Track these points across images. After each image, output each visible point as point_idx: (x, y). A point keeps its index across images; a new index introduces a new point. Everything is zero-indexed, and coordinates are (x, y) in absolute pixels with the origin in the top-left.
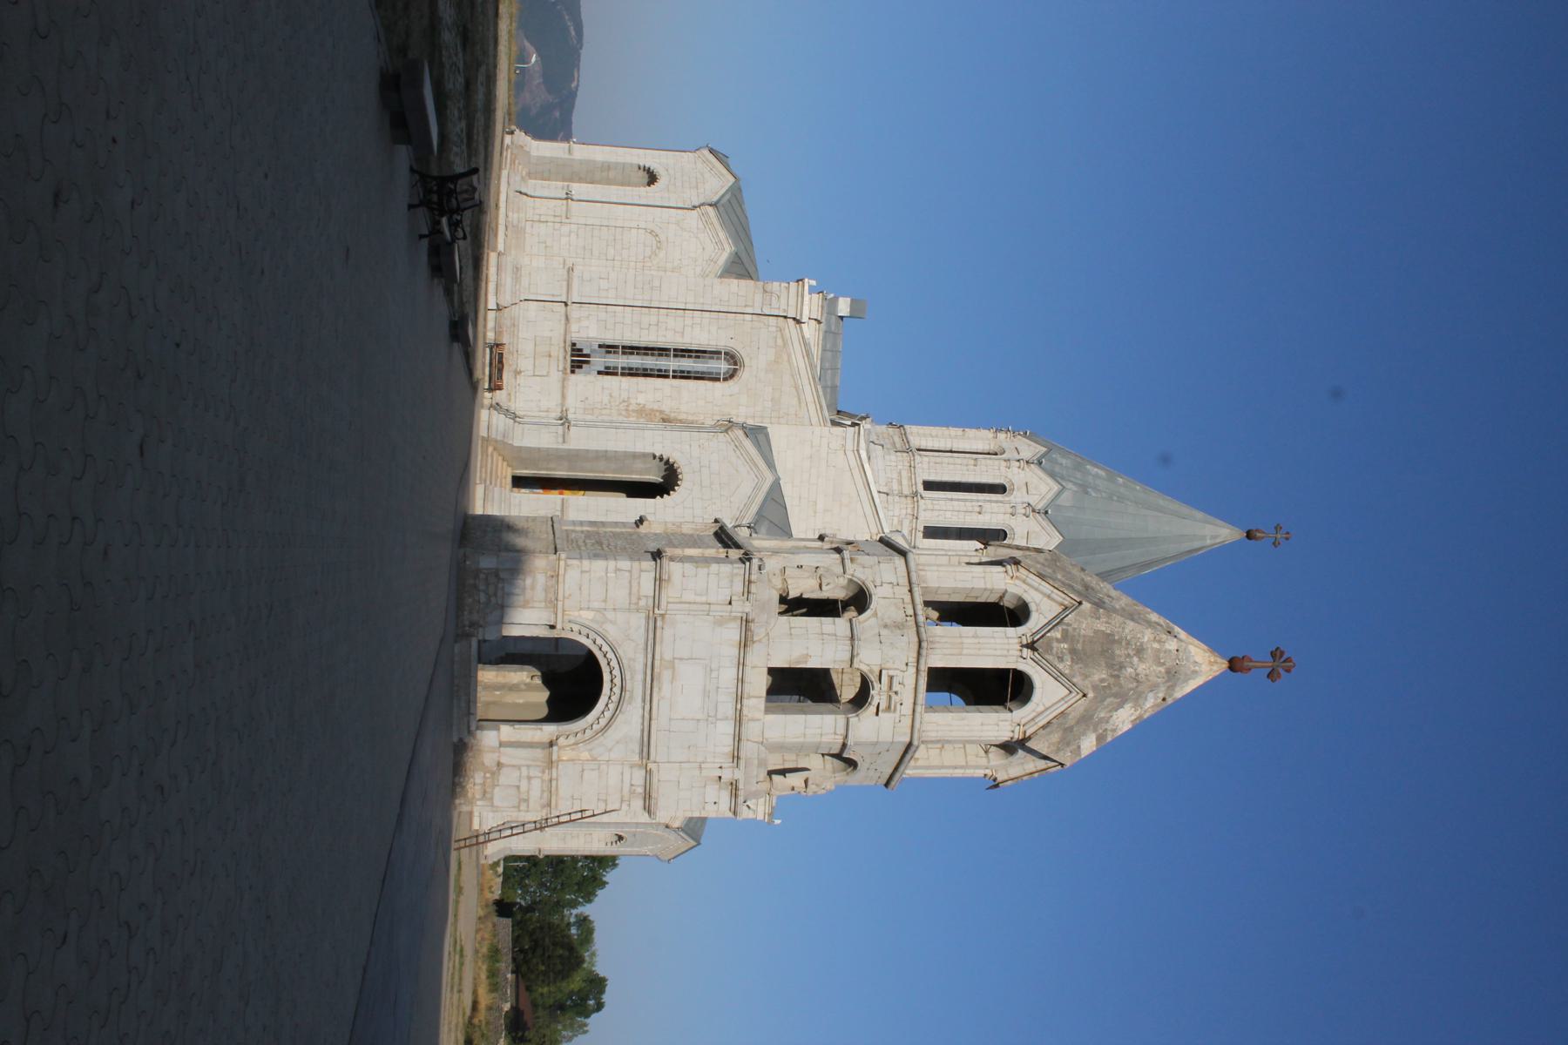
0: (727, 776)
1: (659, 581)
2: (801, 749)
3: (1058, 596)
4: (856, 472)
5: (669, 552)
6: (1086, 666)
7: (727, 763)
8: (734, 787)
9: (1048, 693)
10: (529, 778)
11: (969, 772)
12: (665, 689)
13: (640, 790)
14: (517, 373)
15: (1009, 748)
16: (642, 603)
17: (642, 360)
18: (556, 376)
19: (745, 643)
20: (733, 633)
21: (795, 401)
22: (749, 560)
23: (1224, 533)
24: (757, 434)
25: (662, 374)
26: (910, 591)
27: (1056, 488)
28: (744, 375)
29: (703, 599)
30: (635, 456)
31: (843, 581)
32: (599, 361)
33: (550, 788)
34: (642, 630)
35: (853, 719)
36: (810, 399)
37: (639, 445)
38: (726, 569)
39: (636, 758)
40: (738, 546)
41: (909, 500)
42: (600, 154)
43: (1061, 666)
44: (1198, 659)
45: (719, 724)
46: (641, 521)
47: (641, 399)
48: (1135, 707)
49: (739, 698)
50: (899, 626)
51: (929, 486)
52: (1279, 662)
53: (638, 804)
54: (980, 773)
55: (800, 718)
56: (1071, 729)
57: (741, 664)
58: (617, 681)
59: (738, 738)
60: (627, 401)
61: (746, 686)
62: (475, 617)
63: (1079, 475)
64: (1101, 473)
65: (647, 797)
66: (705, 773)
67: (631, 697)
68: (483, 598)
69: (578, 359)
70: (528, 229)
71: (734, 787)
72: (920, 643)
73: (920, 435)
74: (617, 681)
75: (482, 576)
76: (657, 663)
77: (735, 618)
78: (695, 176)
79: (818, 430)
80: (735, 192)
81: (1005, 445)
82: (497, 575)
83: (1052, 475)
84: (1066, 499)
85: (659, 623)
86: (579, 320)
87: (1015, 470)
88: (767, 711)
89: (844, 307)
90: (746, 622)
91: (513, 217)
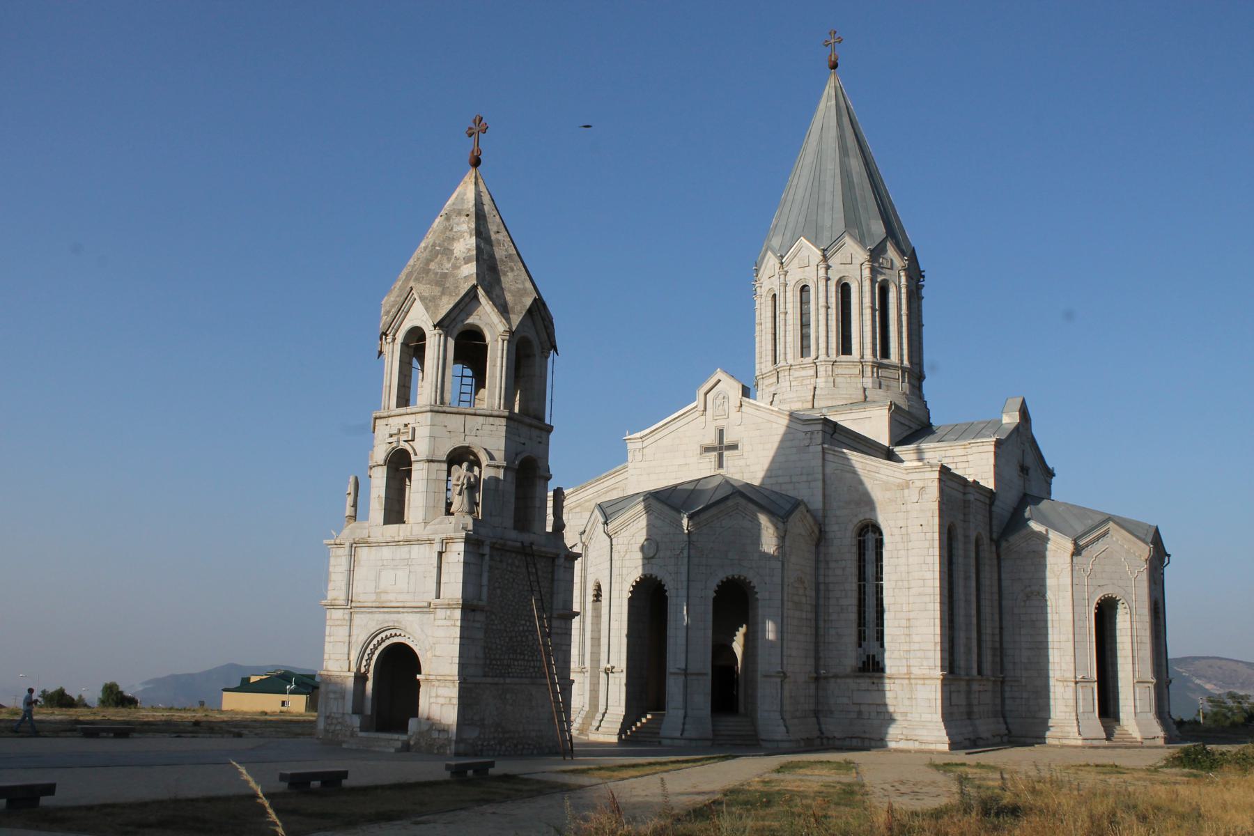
0: (437, 547)
4: (657, 437)
8: (445, 542)
10: (437, 696)
12: (391, 598)
13: (448, 612)
19: (367, 543)
20: (363, 552)
33: (443, 680)
35: (413, 458)
36: (612, 481)
48: (459, 236)
52: (478, 128)
57: (378, 544)
58: (393, 632)
62: (348, 733)
65: (449, 606)
68: (338, 727)
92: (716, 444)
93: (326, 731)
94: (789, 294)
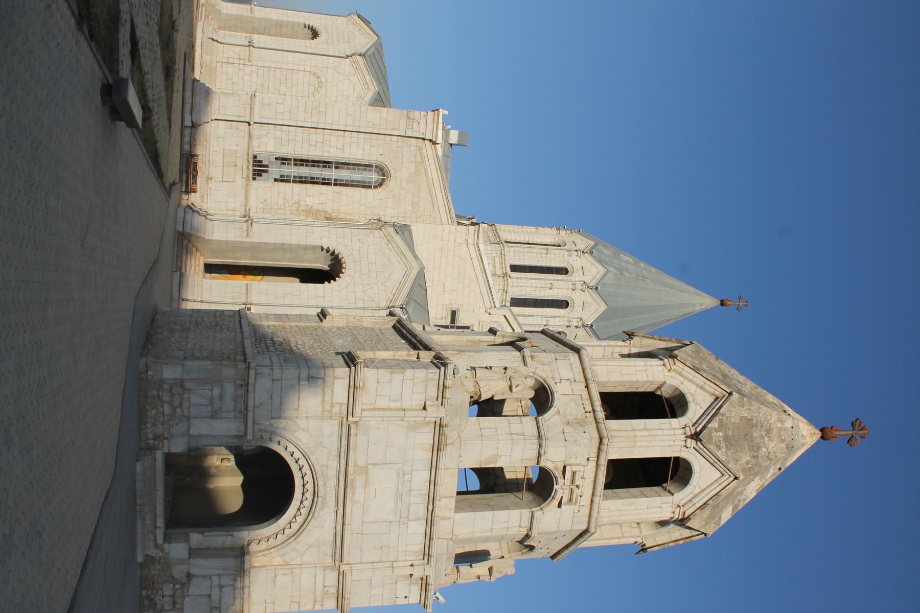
0: (418, 572)
1: (353, 388)
2: (487, 540)
3: (710, 387)
5: (362, 355)
6: (736, 451)
7: (418, 560)
8: (425, 583)
9: (704, 475)
10: (221, 587)
11: (623, 541)
12: (358, 494)
13: (333, 590)
14: (209, 179)
15: (663, 523)
16: (336, 410)
17: (313, 171)
18: (240, 182)
19: (438, 447)
20: (426, 437)
21: (430, 205)
22: (445, 365)
23: (708, 302)
24: (403, 230)
25: (326, 182)
26: (587, 387)
27: (603, 271)
28: (391, 184)
29: (398, 405)
30: (306, 248)
31: (531, 382)
32: (276, 170)
34: (335, 438)
36: (441, 203)
37: (307, 240)
38: (420, 374)
39: (329, 560)
40: (427, 348)
41: (501, 279)
42: (275, 14)
43: (719, 454)
44: (804, 433)
45: (410, 523)
46: (323, 315)
47: (309, 202)
49: (432, 499)
50: (581, 423)
51: (514, 268)
53: (331, 604)
54: (632, 541)
55: (488, 514)
56: (717, 505)
57: (434, 467)
58: (309, 486)
59: (429, 538)
60: (298, 203)
61: (438, 488)
62: (160, 429)
63: (616, 261)
64: (630, 260)
65: (340, 596)
66: (397, 572)
67: (324, 503)
68: (167, 409)
69: (259, 169)
70: (219, 69)
71: (425, 583)
72: (601, 442)
73: (508, 232)
74: (309, 486)
75: (165, 386)
76: (350, 470)
77: (429, 423)
78: (347, 34)
79: (447, 227)
80: (378, 47)
81: (565, 240)
82: (182, 386)
83: (600, 261)
84: (610, 279)
85: (353, 431)
86: (260, 137)
87: (574, 257)
88: (458, 508)
89: (454, 137)
90: (440, 426)
91: (207, 58)
92: (458, 324)
93: (160, 384)
94: (565, 291)
